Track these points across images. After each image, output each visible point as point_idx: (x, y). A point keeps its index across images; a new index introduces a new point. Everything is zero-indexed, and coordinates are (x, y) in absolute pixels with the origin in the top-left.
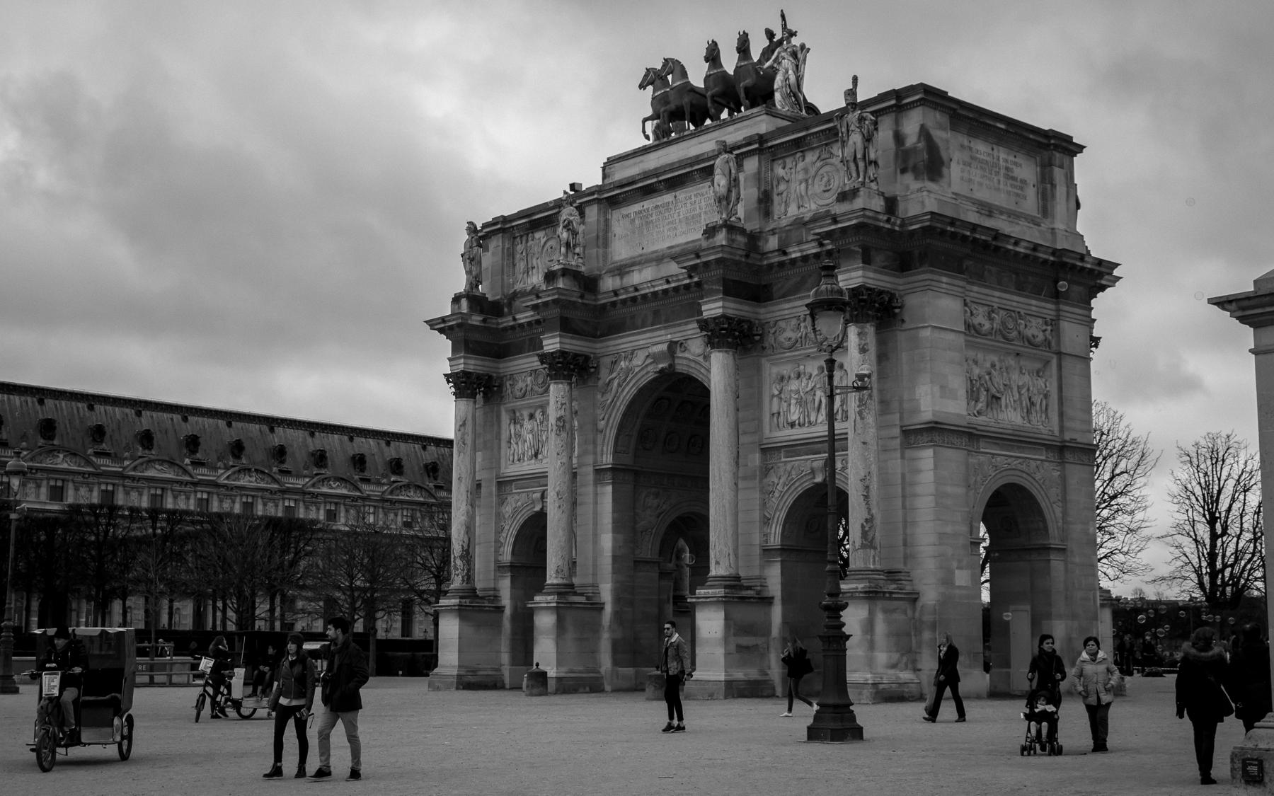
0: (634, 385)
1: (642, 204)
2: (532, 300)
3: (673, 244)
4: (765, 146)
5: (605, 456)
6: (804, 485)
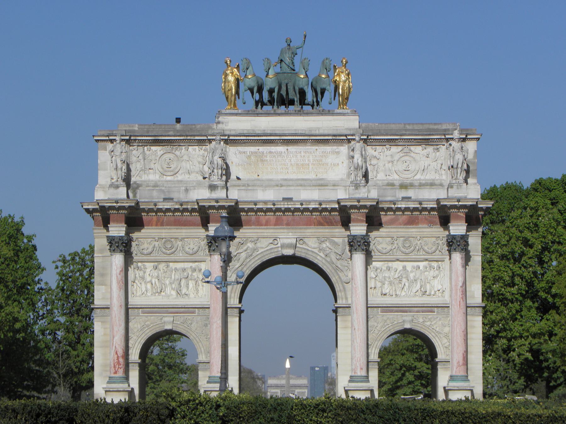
0: (259, 259)
1: (257, 148)
2: (210, 202)
3: (285, 177)
4: (369, 137)
5: (232, 300)
6: (396, 328)
